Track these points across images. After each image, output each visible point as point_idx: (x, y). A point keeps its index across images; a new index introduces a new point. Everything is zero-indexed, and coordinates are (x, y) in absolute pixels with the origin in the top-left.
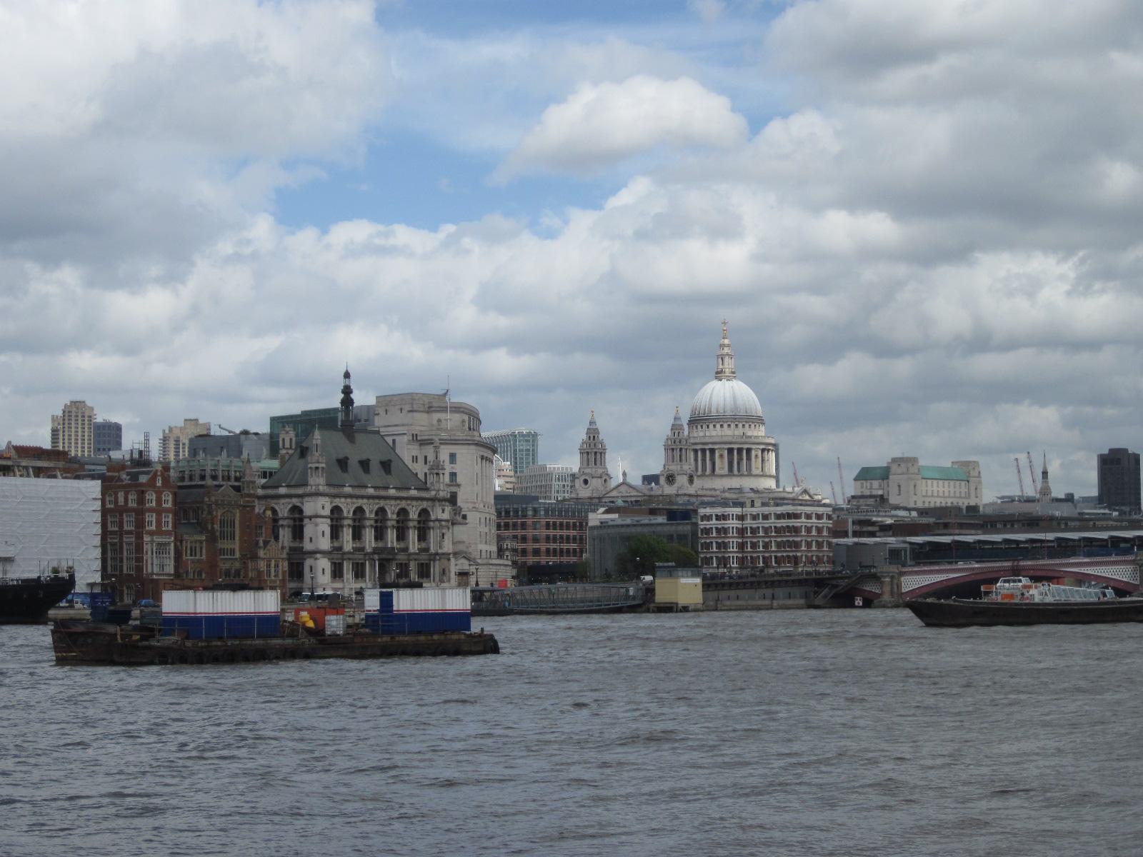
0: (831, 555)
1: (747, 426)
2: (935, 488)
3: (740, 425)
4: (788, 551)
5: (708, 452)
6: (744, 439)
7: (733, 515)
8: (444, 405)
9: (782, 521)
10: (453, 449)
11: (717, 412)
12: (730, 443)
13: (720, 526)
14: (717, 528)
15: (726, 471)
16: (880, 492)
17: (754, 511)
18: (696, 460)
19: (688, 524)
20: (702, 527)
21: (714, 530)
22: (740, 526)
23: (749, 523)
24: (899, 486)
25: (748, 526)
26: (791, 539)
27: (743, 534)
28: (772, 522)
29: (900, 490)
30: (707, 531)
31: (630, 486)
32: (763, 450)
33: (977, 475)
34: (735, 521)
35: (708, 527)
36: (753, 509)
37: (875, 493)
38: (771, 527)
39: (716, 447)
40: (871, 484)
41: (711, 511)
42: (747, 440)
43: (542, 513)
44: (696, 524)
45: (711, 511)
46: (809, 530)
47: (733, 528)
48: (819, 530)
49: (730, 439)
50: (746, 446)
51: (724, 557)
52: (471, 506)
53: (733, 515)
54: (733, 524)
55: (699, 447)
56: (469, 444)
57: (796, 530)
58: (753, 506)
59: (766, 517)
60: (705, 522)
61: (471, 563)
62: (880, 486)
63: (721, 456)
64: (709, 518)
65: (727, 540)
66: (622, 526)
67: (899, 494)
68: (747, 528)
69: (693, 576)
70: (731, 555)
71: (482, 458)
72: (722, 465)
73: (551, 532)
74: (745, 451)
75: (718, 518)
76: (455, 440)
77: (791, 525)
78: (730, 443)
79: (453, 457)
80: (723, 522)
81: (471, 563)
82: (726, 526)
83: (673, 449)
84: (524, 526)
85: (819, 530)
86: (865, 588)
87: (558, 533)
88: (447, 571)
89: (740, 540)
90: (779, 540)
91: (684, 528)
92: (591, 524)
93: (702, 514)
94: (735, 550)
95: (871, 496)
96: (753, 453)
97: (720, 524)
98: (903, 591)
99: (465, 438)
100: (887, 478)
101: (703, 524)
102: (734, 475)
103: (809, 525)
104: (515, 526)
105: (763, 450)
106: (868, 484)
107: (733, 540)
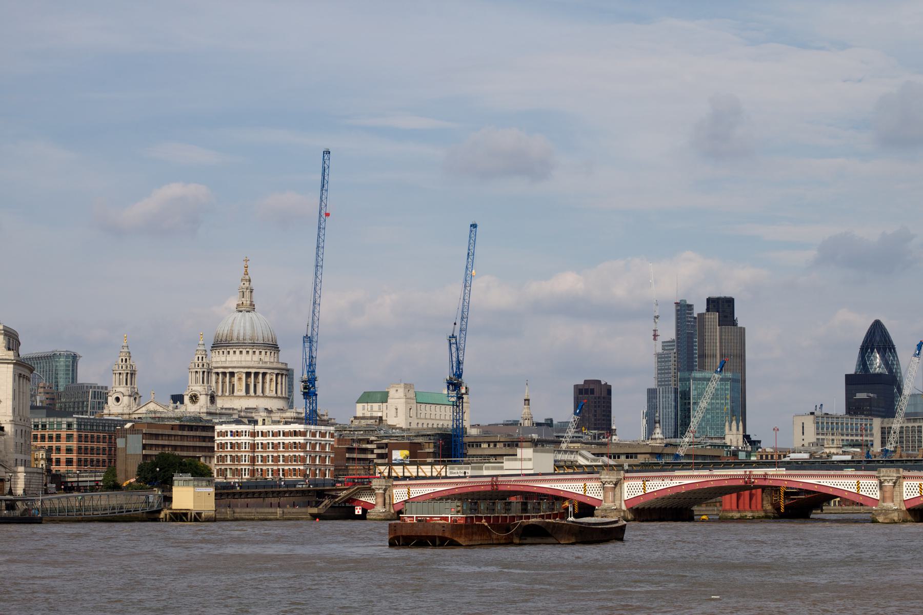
2: (428, 412)
3: (257, 352)
5: (228, 375)
6: (261, 365)
7: (246, 432)
9: (290, 438)
11: (238, 339)
12: (249, 368)
13: (234, 442)
14: (231, 443)
15: (243, 393)
16: (380, 414)
20: (218, 442)
22: (252, 442)
23: (259, 439)
24: (397, 409)
25: (259, 442)
29: (397, 413)
32: (277, 375)
34: (247, 437)
35: (223, 442)
36: (264, 427)
37: (375, 414)
39: (235, 370)
40: (372, 406)
42: (264, 365)
43: (75, 426)
47: (245, 443)
48: (323, 447)
49: (251, 365)
50: (262, 371)
51: (237, 469)
53: (246, 432)
57: (303, 446)
58: (264, 424)
60: (221, 438)
61: (8, 470)
63: (240, 379)
65: (239, 454)
68: (258, 444)
70: (243, 467)
71: (20, 375)
72: (240, 389)
74: (260, 376)
77: (297, 441)
78: (249, 368)
80: (237, 438)
81: (8, 470)
82: (239, 442)
83: (196, 372)
84: (58, 437)
93: (218, 431)
94: (247, 463)
95: (371, 418)
96: (268, 377)
97: (234, 439)
98: (395, 502)
99: (4, 357)
102: (250, 396)
104: (51, 438)
105: (277, 375)
106: (369, 407)
107: (245, 453)
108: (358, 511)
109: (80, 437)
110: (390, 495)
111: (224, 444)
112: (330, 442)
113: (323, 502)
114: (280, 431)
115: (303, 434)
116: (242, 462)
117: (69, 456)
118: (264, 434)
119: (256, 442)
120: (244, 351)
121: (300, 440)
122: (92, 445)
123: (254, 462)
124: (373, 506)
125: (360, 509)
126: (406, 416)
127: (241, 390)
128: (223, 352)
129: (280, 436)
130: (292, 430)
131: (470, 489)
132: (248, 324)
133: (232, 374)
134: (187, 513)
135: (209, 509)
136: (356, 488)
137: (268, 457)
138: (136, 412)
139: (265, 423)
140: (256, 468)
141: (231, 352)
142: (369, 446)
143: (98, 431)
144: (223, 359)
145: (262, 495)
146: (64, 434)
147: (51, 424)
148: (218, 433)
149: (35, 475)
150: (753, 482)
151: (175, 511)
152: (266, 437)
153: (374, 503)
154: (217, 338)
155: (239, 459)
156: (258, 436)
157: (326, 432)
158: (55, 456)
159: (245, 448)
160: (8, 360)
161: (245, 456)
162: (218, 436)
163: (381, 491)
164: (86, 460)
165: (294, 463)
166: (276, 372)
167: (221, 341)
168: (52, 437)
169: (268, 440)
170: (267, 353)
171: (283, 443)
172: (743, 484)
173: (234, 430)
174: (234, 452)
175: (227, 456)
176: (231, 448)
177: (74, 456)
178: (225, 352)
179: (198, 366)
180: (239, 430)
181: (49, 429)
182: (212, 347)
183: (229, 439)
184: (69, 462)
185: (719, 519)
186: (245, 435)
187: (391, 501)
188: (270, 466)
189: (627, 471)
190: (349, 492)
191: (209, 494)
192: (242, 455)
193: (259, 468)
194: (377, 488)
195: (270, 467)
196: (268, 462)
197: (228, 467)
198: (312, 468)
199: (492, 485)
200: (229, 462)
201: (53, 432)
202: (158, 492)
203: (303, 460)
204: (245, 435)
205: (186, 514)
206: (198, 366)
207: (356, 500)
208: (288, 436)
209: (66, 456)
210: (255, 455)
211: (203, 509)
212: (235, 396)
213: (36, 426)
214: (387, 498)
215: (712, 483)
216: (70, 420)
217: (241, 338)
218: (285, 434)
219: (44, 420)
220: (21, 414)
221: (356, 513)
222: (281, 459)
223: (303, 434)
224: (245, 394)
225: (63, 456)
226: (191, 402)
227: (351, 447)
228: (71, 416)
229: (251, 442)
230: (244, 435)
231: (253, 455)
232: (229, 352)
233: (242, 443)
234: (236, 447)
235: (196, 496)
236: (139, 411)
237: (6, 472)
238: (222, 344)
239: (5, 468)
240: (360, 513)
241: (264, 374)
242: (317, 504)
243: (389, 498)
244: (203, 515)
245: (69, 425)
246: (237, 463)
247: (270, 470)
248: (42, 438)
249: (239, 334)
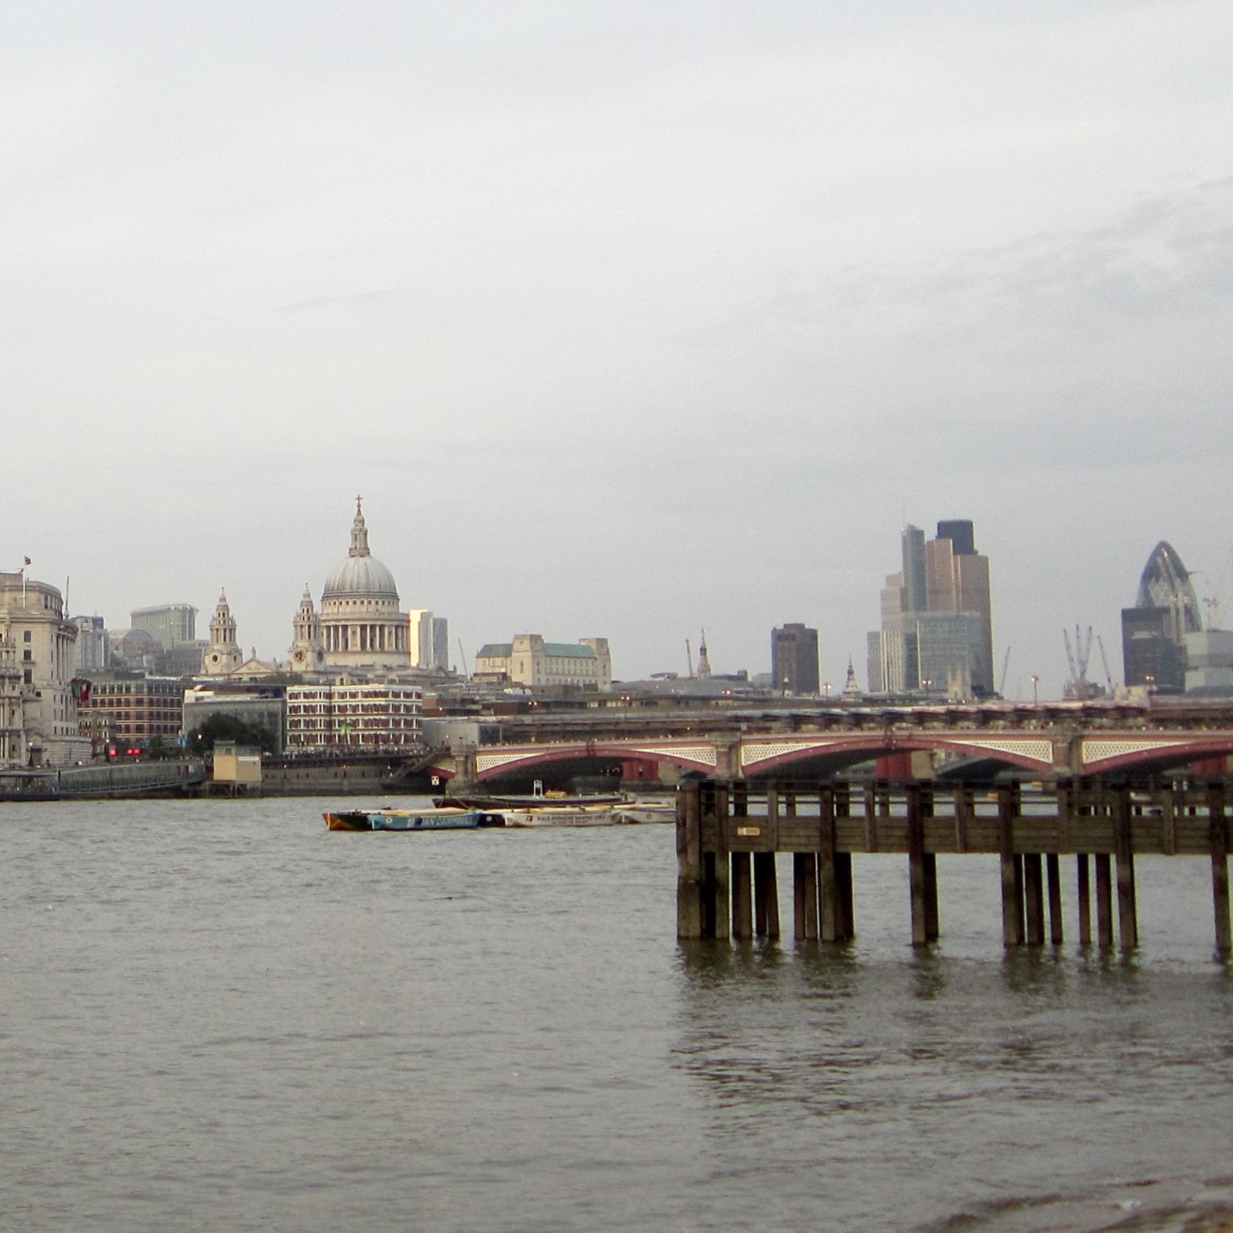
0: (421, 733)
1: (380, 603)
3: (373, 602)
4: (376, 730)
7: (320, 693)
8: (19, 584)
9: (370, 699)
10: (27, 627)
11: (351, 587)
13: (307, 705)
14: (305, 706)
15: (358, 648)
16: (503, 670)
17: (341, 689)
18: (329, 636)
19: (278, 701)
20: (290, 705)
21: (302, 708)
23: (337, 701)
24: (522, 664)
25: (336, 704)
26: (378, 717)
27: (331, 712)
28: (360, 701)
30: (295, 709)
31: (258, 662)
33: (605, 652)
34: (322, 699)
35: (296, 705)
36: (341, 687)
37: (497, 670)
38: (358, 705)
39: (348, 623)
41: (299, 689)
42: (381, 616)
44: (284, 702)
45: (299, 689)
46: (396, 708)
48: (408, 709)
49: (367, 616)
50: (379, 623)
51: (312, 735)
52: (45, 683)
53: (320, 693)
54: (320, 702)
55: (333, 623)
56: (44, 623)
57: (384, 709)
59: (354, 695)
60: (294, 700)
62: (503, 664)
63: (354, 633)
64: (294, 696)
66: (215, 703)
67: (522, 672)
68: (335, 706)
69: (253, 753)
72: (355, 643)
73: (155, 709)
74: (378, 629)
75: (306, 696)
76: (31, 618)
77: (378, 703)
79: (27, 637)
82: (313, 704)
85: (408, 709)
86: (440, 767)
87: (162, 710)
88: (17, 747)
89: (328, 718)
90: (366, 718)
91: (275, 706)
92: (186, 701)
94: (322, 727)
95: (493, 674)
98: (478, 771)
100: (510, 655)
101: (291, 702)
102: (367, 652)
103: (397, 704)
105: (397, 627)
107: (320, 719)
108: (435, 781)
115: (385, 695)
117: (139, 722)
119: (333, 704)
120: (358, 602)
121: (381, 701)
124: (453, 775)
126: (533, 672)
128: (335, 603)
131: (561, 756)
132: (362, 572)
140: (333, 733)
141: (344, 603)
142: (474, 707)
150: (896, 744)
155: (314, 723)
162: (290, 698)
163: (462, 759)
166: (395, 623)
168: (112, 702)
172: (884, 746)
173: (307, 692)
174: (309, 715)
183: (302, 701)
185: (644, 786)
189: (745, 733)
195: (360, 733)
199: (588, 750)
200: (302, 727)
203: (386, 723)
205: (227, 786)
212: (350, 652)
214: (469, 765)
215: (845, 745)
216: (140, 682)
219: (112, 683)
221: (433, 783)
223: (385, 695)
229: (326, 704)
239: (42, 737)
240: (438, 783)
241: (381, 627)
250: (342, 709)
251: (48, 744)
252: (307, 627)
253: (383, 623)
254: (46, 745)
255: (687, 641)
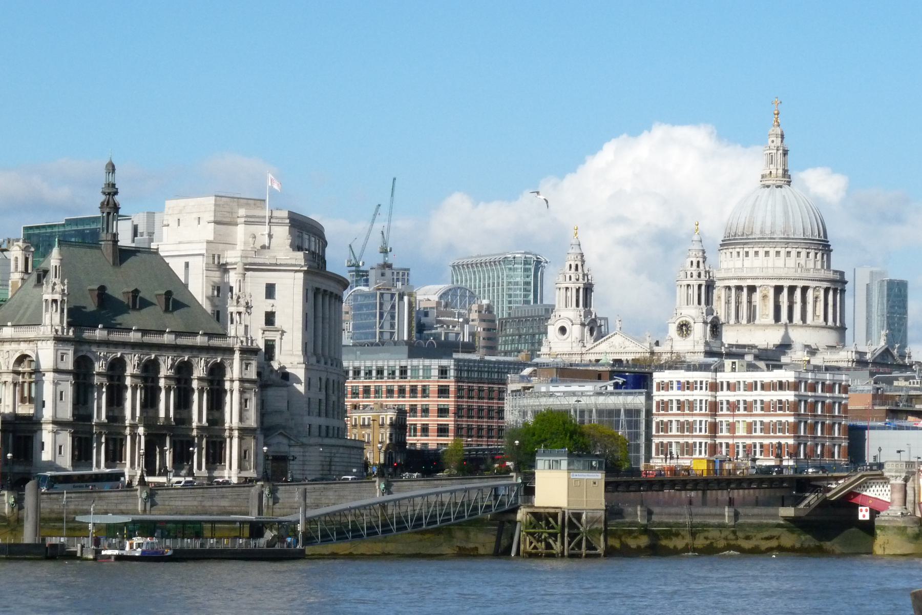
3: (794, 253)
7: (701, 383)
9: (772, 392)
10: (270, 277)
11: (762, 232)
13: (682, 399)
14: (678, 401)
15: (770, 319)
18: (728, 302)
22: (713, 399)
23: (723, 396)
30: (665, 406)
35: (666, 399)
39: (757, 283)
42: (805, 275)
43: (452, 373)
47: (701, 401)
49: (782, 273)
53: (701, 383)
54: (701, 395)
56: (296, 271)
58: (733, 370)
63: (765, 297)
71: (317, 291)
72: (765, 311)
75: (682, 386)
76: (276, 265)
77: (784, 399)
79: (270, 291)
80: (687, 392)
84: (425, 390)
91: (637, 400)
96: (810, 294)
99: (289, 262)
105: (827, 291)
107: (701, 419)
108: (864, 514)
109: (459, 389)
110: (914, 488)
111: (668, 402)
112: (840, 400)
113: (806, 498)
114: (756, 382)
116: (696, 431)
117: (443, 421)
118: (731, 386)
120: (772, 252)
122: (470, 402)
123: (715, 433)
124: (886, 505)
125: (866, 511)
127: (767, 315)
128: (738, 253)
129: (756, 389)
130: (775, 380)
132: (779, 209)
133: (752, 289)
134: (556, 514)
135: (594, 508)
136: (859, 475)
137: (755, 425)
138: (591, 351)
139: (735, 368)
140: (718, 441)
143: (480, 381)
144: (739, 264)
145: (701, 486)
146: (433, 386)
147: (415, 369)
148: (658, 384)
149: (341, 450)
151: (536, 510)
152: (735, 390)
153: (889, 501)
154: (728, 231)
156: (722, 390)
157: (834, 384)
158: (420, 420)
159: (701, 409)
160: (295, 265)
161: (701, 422)
164: (470, 428)
165: (778, 434)
166: (825, 285)
167: (735, 236)
169: (738, 395)
170: (733, 254)
171: (762, 402)
173: (682, 380)
174: (683, 415)
175: (671, 422)
176: (679, 409)
177: (449, 421)
178: (741, 254)
179: (692, 277)
180: (691, 380)
181: (412, 377)
182: (721, 245)
183: (674, 395)
184: (442, 430)
186: (701, 388)
187: (917, 498)
188: (741, 438)
190: (848, 482)
191: (595, 483)
192: (695, 421)
193: (724, 441)
194: (892, 476)
196: (755, 432)
197: (673, 440)
198: (843, 444)
200: (674, 432)
201: (417, 381)
202: (516, 480)
204: (701, 388)
205: (555, 516)
206: (692, 277)
207: (859, 494)
208: (770, 390)
209: (437, 421)
210: (717, 420)
211: (585, 507)
212: (758, 325)
213: (357, 372)
216: (444, 362)
217: (768, 232)
218: (764, 387)
219: (403, 363)
220: (320, 351)
221: (861, 518)
222: (758, 427)
224: (773, 322)
225: (433, 421)
226: (679, 335)
227: (895, 408)
228: (449, 356)
230: (699, 388)
231: (713, 420)
232: (747, 253)
233: (696, 400)
234: (686, 408)
235: (572, 487)
236: (596, 350)
237: (290, 446)
238: (737, 239)
239: (289, 439)
240: (867, 518)
241: (805, 289)
242: (796, 502)
243: (912, 492)
244: (584, 516)
245: (443, 372)
246: (688, 434)
247: (758, 446)
248: (365, 393)
249: (763, 223)
250: (733, 407)
251: (296, 449)
252: (696, 288)
253: (806, 283)
254: (296, 451)
255: (395, 179)
